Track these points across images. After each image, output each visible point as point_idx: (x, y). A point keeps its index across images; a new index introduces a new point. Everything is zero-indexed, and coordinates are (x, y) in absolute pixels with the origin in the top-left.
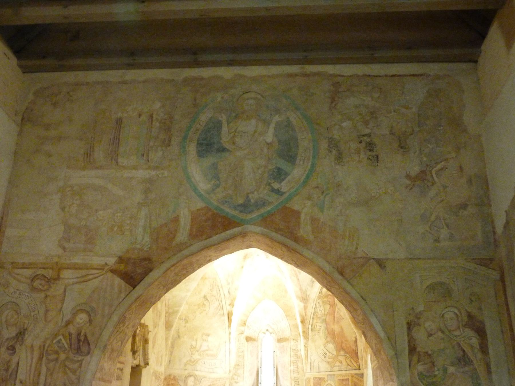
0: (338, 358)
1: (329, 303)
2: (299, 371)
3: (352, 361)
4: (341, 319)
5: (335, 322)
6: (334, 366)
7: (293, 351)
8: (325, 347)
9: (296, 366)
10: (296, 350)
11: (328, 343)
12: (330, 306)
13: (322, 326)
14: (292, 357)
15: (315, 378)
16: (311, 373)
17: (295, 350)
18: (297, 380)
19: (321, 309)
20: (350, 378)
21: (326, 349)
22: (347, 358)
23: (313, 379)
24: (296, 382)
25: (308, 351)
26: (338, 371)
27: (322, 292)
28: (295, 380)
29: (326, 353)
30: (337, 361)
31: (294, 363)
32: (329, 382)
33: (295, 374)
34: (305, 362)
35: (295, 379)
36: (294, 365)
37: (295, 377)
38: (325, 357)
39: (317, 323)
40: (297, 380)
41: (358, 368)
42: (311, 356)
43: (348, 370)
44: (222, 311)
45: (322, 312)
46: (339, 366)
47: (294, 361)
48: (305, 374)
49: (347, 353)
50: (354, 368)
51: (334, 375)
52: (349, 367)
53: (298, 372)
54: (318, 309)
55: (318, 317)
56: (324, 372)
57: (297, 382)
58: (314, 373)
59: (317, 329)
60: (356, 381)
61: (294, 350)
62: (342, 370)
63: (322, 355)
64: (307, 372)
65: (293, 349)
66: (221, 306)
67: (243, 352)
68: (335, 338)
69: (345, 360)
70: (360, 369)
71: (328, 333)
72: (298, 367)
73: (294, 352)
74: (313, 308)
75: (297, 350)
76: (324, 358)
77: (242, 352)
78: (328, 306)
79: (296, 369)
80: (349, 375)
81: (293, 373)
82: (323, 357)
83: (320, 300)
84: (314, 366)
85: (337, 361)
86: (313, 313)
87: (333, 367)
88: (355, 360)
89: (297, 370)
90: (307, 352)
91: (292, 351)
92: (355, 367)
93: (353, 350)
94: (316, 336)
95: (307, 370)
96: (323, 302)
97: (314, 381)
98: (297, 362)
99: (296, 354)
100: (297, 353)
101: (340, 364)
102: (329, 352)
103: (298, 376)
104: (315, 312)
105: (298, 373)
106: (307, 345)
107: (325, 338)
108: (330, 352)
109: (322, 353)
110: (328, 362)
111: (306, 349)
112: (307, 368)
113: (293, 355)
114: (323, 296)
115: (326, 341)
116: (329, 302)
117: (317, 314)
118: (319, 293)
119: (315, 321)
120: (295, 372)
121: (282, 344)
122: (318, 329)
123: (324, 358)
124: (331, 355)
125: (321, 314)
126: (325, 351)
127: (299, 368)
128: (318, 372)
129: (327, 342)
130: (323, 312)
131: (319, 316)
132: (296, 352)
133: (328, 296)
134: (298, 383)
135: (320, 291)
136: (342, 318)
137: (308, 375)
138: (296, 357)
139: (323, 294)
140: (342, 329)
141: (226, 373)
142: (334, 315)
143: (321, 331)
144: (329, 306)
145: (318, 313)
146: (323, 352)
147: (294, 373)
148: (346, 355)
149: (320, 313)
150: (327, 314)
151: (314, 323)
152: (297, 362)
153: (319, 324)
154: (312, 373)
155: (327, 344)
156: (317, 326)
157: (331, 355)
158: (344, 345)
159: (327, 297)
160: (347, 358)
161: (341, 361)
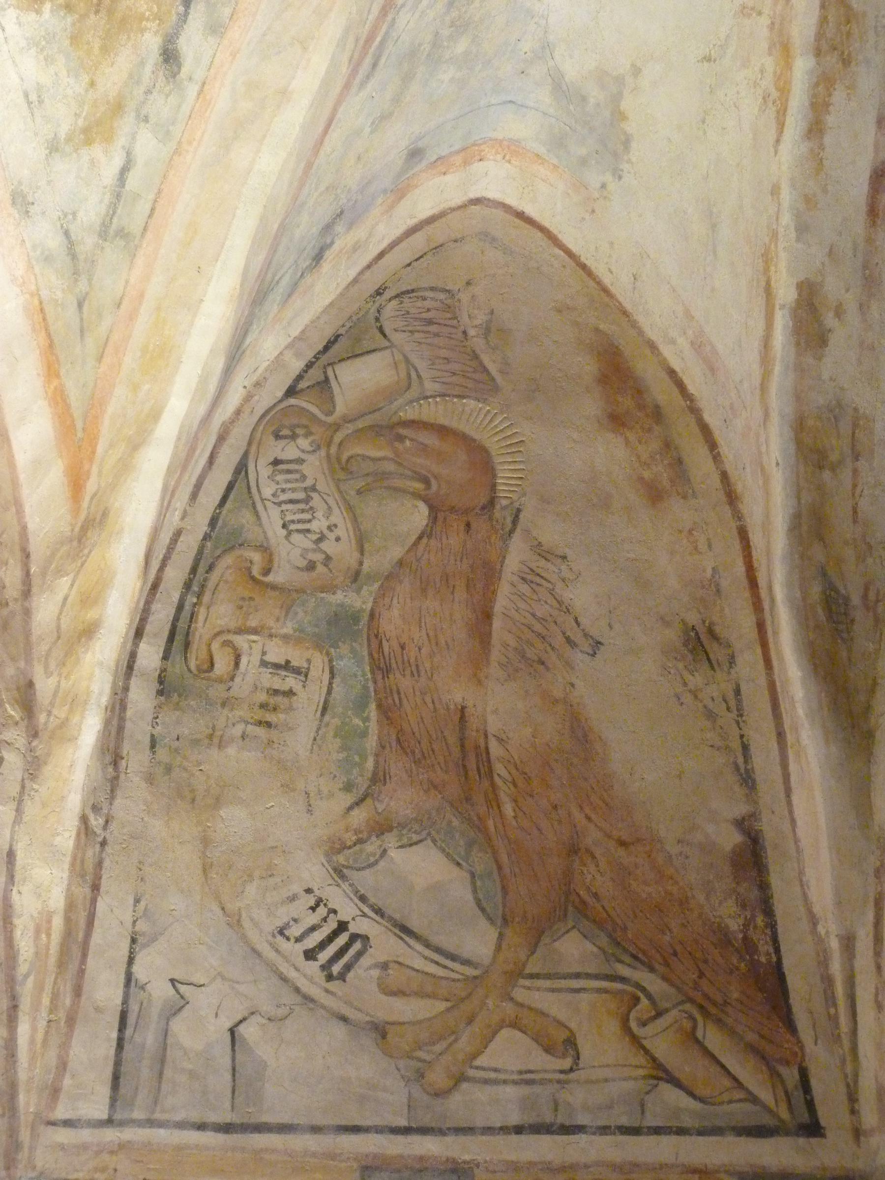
1: (419, 486)
3: (713, 1038)
5: (496, 654)
6: (461, 1078)
8: (339, 872)
11: (390, 840)
13: (319, 662)
16: (110, 1135)
21: (363, 898)
22: (644, 1002)
25: (96, 888)
26: (519, 1130)
27: (324, 384)
29: (353, 928)
30: (502, 1025)
34: (55, 997)
38: (342, 977)
39: (239, 631)
41: (785, 1114)
42: (133, 941)
43: (657, 1131)
46: (526, 1079)
48: (25, 1135)
49: (638, 959)
50: (742, 1112)
54: (272, 518)
55: (274, 587)
56: (316, 1129)
58: (161, 1135)
59: (241, 687)
62: (582, 1119)
64: (61, 1112)
68: (493, 801)
69: (613, 1026)
76: (330, 978)
82: (313, 968)
84: (162, 1060)
85: (514, 1025)
87: (438, 1077)
88: (751, 1037)
90: (88, 890)
92: (754, 1099)
93: (724, 939)
94: (231, 751)
95: (55, 1092)
101: (539, 1060)
106: (101, 821)
107: (348, 787)
108: (414, 924)
109: (295, 931)
111: (91, 854)
112: (63, 1066)
115: (359, 816)
116: (426, 482)
118: (291, 392)
122: (262, 697)
123: (320, 977)
125: (311, 566)
126: (347, 910)
128: (227, 1128)
131: (276, 577)
135: (300, 377)
136: (577, 637)
139: (341, 408)
144: (424, 509)
145: (265, 549)
146: (313, 919)
148: (623, 971)
150: (390, 578)
151: (202, 630)
154: (128, 1134)
155: (372, 847)
157: (418, 963)
159: (401, 438)
160: (644, 1002)
161: (563, 1035)
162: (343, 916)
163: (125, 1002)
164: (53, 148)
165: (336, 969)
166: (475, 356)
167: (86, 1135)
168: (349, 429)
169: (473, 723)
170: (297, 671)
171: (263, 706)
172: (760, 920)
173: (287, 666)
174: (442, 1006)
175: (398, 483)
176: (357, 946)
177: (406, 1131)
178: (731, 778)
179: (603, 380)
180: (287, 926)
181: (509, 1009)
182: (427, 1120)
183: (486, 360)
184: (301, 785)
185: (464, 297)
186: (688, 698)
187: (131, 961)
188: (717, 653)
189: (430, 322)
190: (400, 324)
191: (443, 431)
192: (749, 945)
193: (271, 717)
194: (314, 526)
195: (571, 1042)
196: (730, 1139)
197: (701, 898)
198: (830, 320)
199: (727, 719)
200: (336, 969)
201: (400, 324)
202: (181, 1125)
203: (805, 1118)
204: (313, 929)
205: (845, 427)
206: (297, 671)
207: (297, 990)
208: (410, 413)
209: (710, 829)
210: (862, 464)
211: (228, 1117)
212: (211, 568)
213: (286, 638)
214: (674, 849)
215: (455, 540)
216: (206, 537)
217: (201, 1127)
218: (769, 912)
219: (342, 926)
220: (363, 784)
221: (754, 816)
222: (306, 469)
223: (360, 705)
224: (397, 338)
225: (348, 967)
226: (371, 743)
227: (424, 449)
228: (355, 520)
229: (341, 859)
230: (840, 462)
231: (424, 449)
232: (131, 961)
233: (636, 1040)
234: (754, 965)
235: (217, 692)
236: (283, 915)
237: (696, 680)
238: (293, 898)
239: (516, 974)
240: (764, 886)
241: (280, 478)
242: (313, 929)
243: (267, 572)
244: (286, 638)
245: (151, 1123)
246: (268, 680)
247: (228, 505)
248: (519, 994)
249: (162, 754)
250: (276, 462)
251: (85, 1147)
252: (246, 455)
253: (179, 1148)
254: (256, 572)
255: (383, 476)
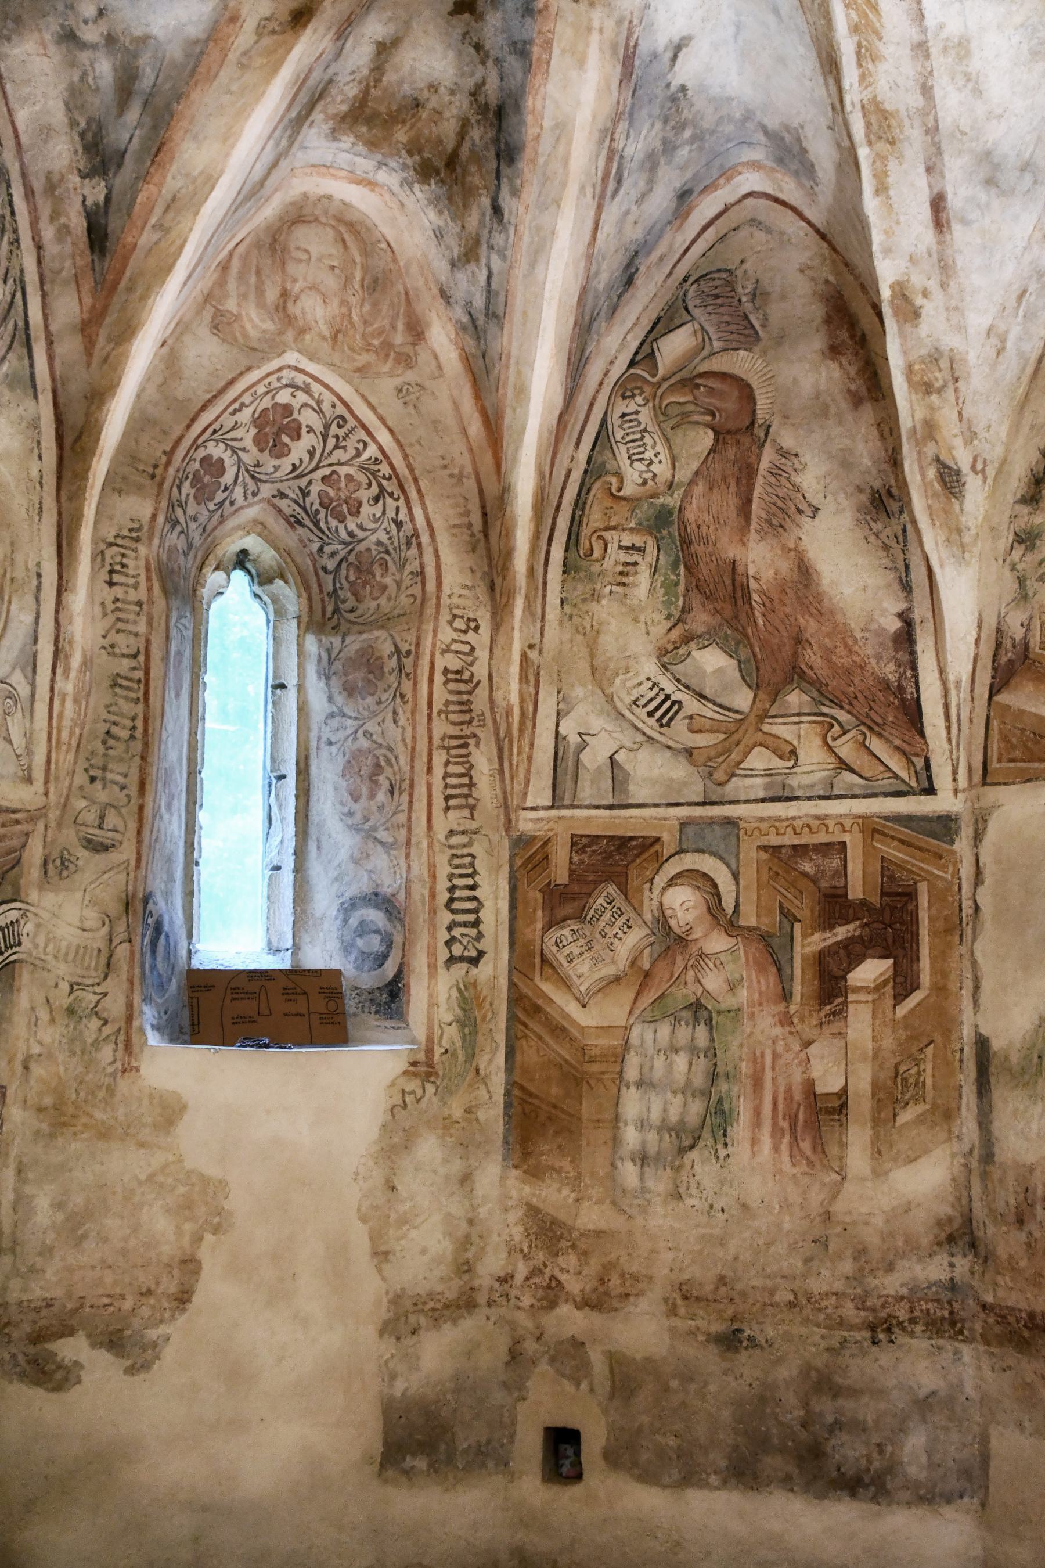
0: (766, 728)
2: (477, 800)
3: (876, 744)
4: (800, 511)
5: (754, 525)
6: (734, 775)
7: (445, 683)
8: (665, 667)
9: (460, 770)
10: (466, 675)
11: (693, 645)
12: (716, 440)
13: (651, 542)
14: (439, 713)
15: (579, 843)
16: (554, 813)
17: (458, 677)
18: (465, 846)
19: (649, 454)
20: (853, 840)
21: (678, 681)
22: (837, 727)
23: (573, 844)
24: (456, 861)
26: (763, 800)
27: (652, 355)
28: (451, 847)
29: (673, 698)
31: (448, 749)
32: (708, 864)
33: (451, 813)
35: (455, 840)
36: (447, 763)
37: (451, 833)
38: (668, 725)
39: (607, 529)
40: (465, 846)
41: (914, 784)
42: (558, 714)
44: (26, 362)
45: (655, 468)
46: (768, 774)
47: (451, 737)
51: (730, 822)
52: (848, 777)
53: (471, 801)
54: (622, 453)
55: (623, 499)
56: (656, 806)
57: (463, 856)
58: (578, 812)
60: (896, 853)
61: (450, 676)
62: (798, 794)
63: (643, 713)
64: (529, 804)
65: (446, 671)
66: (21, 324)
67: (141, 658)
69: (818, 741)
70: (930, 790)
71: (697, 585)
72: (473, 772)
73: (452, 686)
74: (577, 445)
75: (471, 680)
76: (661, 726)
77: (135, 656)
78: (706, 439)
79: (461, 786)
80: (848, 823)
81: (444, 805)
82: (652, 721)
83: (639, 400)
86: (576, 476)
88: (897, 742)
89: (465, 791)
91: (439, 678)
92: (896, 776)
93: (886, 685)
96: (661, 413)
97: (576, 859)
98: (465, 745)
99: (465, 697)
100: (470, 693)
102: (701, 696)
103: (473, 825)
104: (594, 470)
105: (472, 808)
107: (668, 617)
108: (707, 692)
110: (689, 752)
113: (447, 703)
114: (665, 379)
115: (675, 634)
116: (713, 415)
117: (614, 480)
118: (632, 364)
119: (595, 518)
120: (452, 802)
121: (354, 643)
122: (620, 568)
123: (656, 726)
124: (709, 711)
125: (645, 482)
126: (669, 687)
127: (474, 780)
129: (687, 639)
130: (662, 469)
132: (462, 687)
133: (698, 381)
134: (472, 865)
135: (636, 353)
136: (803, 506)
137: (526, 823)
138: (467, 717)
139: (661, 371)
140: (804, 571)
141: (29, 780)
142: (751, 488)
143: (643, 579)
144: (711, 433)
145: (619, 475)
146: (652, 694)
147: (448, 808)
148: (825, 710)
149: (633, 475)
150: (692, 483)
151: (586, 531)
152: (465, 745)
153: (627, 540)
155: (681, 651)
156: (612, 547)
158: (812, 658)
159: (697, 386)
160: (837, 727)
161: (789, 748)
162: (667, 692)
163: (556, 746)
164: (453, 265)
165: (665, 721)
166: (746, 317)
167: (542, 814)
168: (665, 386)
169: (740, 570)
170: (639, 550)
171: (621, 573)
172: (909, 674)
173: (633, 547)
174: (722, 736)
175: (696, 418)
176: (676, 707)
177: (704, 804)
178: (896, 587)
179: (828, 320)
180: (637, 699)
181: (759, 737)
182: (714, 798)
183: (753, 319)
184: (642, 618)
185: (739, 273)
186: (872, 538)
187: (557, 725)
188: (893, 506)
189: (717, 297)
190: (698, 302)
191: (723, 376)
192: (901, 688)
193: (624, 580)
194: (646, 455)
195: (793, 753)
196: (881, 799)
197: (873, 662)
198: (919, 301)
199: (896, 549)
200: (665, 721)
201: (698, 302)
202: (587, 807)
203: (926, 785)
204: (651, 700)
205: (944, 364)
206: (639, 550)
207: (644, 734)
208: (704, 367)
209: (882, 620)
210: (960, 384)
211: (610, 801)
212: (589, 490)
213: (632, 530)
214: (858, 635)
215: (731, 453)
216: (586, 471)
217: (598, 807)
218: (914, 668)
219: (667, 697)
220: (677, 614)
221: (909, 609)
222: (641, 417)
223: (675, 565)
224: (697, 312)
225: (671, 719)
226: (681, 588)
227: (711, 391)
228: (670, 448)
229: (665, 659)
230: (945, 386)
231: (711, 391)
232: (557, 725)
233: (830, 749)
234: (903, 701)
235: (596, 568)
236: (635, 693)
237: (877, 527)
238: (640, 684)
239: (763, 716)
240: (913, 653)
241: (626, 426)
242: (651, 700)
243: (620, 489)
244: (632, 530)
245: (573, 806)
246: (623, 557)
247: (597, 449)
248: (766, 728)
249: (567, 608)
250: (624, 415)
251: (542, 819)
252: (606, 413)
253: (588, 818)
254: (614, 491)
255: (688, 414)
